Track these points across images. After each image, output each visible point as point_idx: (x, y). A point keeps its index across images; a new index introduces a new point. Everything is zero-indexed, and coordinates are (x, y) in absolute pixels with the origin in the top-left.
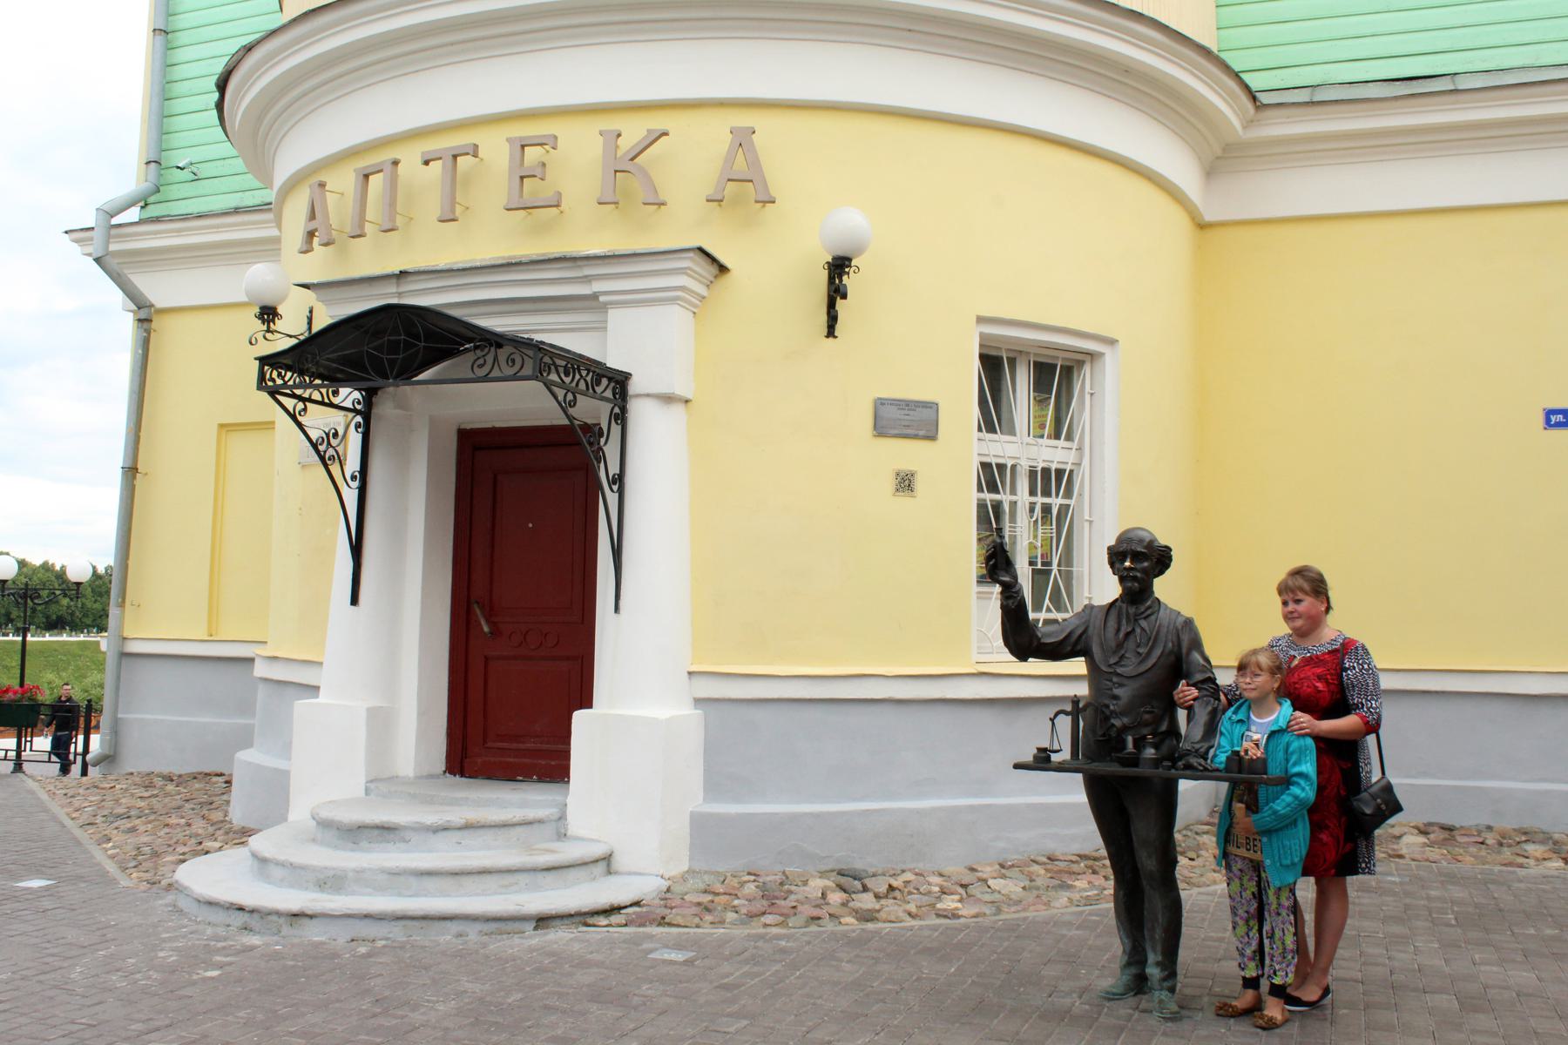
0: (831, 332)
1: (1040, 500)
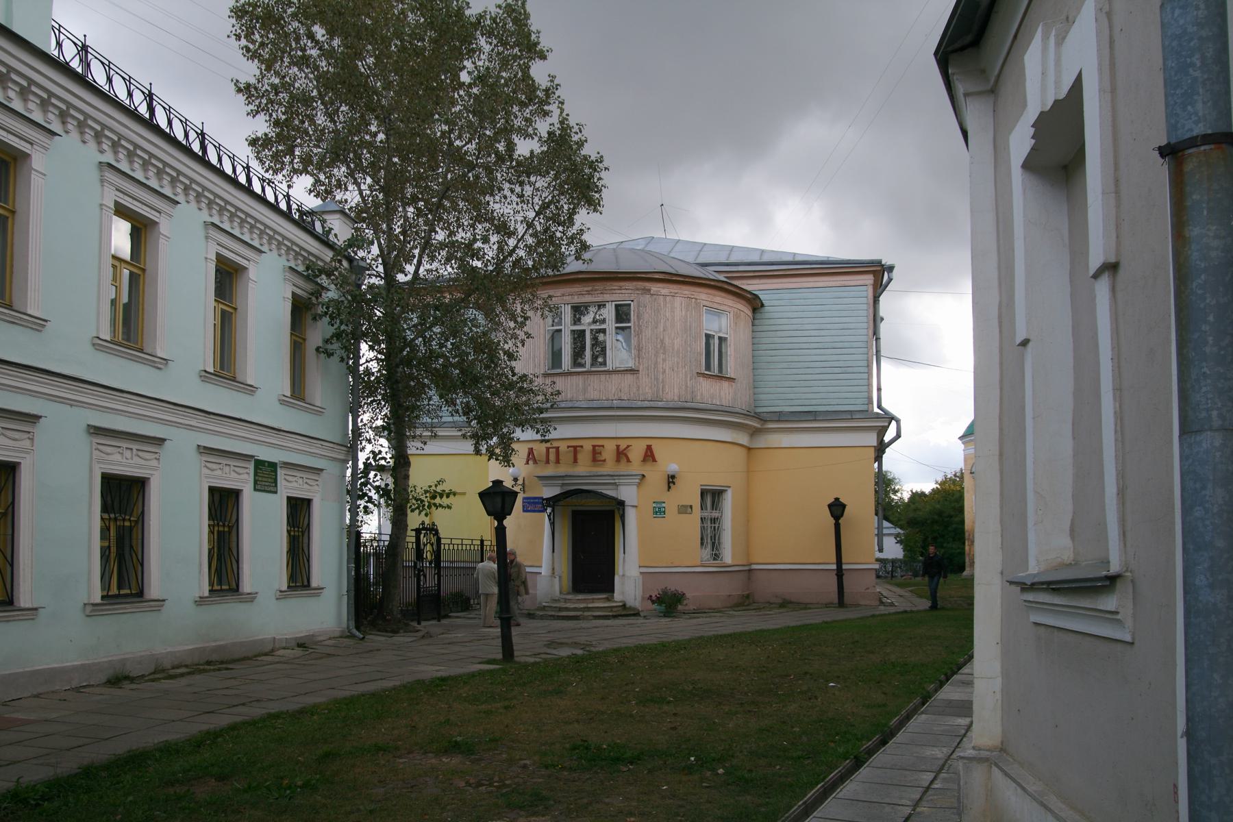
1: (713, 525)
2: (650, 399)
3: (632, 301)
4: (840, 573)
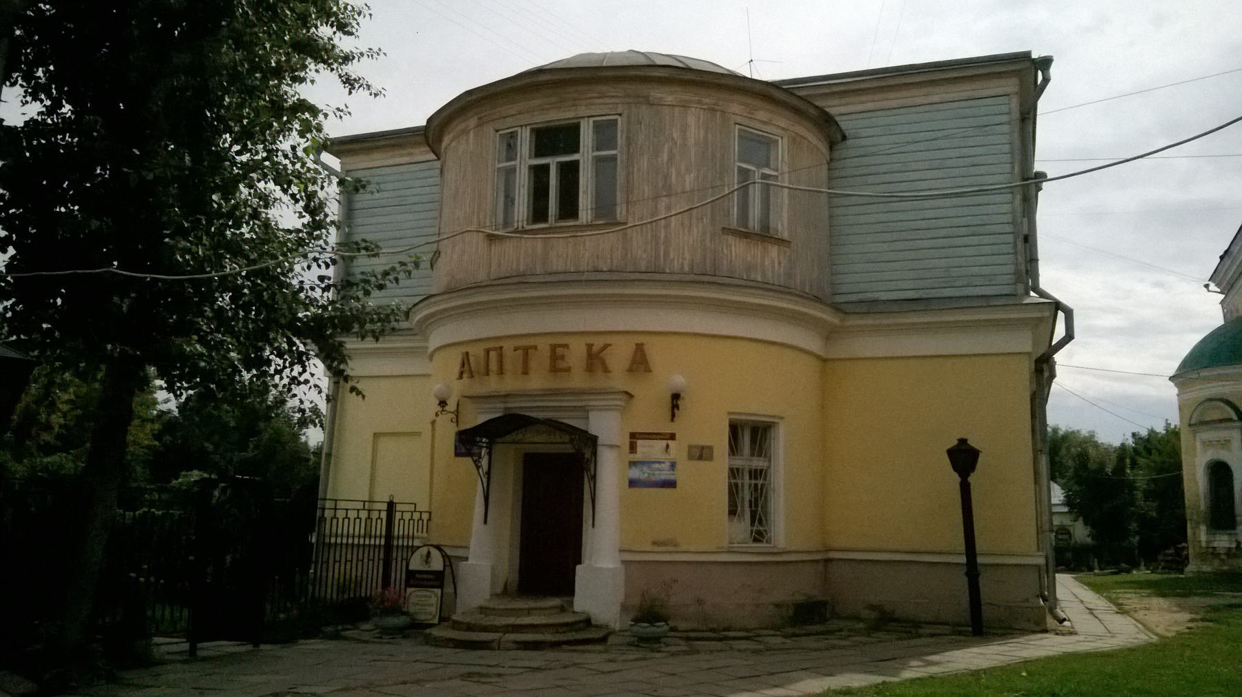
0: (672, 420)
1: (753, 482)
2: (643, 269)
3: (620, 115)
4: (972, 570)
